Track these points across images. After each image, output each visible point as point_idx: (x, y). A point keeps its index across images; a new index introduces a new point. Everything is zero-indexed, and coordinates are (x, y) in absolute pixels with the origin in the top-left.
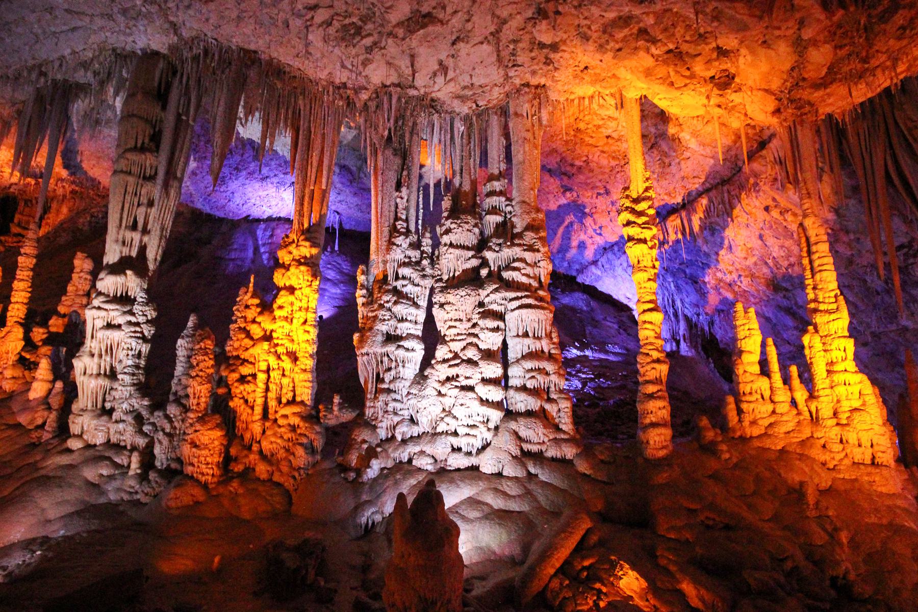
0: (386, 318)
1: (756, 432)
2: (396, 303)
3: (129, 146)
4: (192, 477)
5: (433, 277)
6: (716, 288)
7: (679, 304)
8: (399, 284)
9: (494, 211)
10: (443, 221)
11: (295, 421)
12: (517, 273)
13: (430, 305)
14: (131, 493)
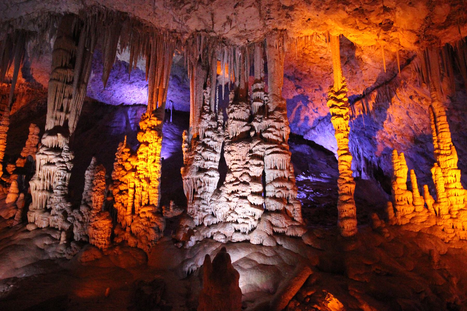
0: (199, 159)
1: (404, 222)
2: (204, 151)
3: (58, 66)
4: (94, 245)
5: (224, 136)
6: (382, 142)
7: (361, 151)
8: (205, 140)
9: (258, 100)
10: (229, 105)
11: (149, 215)
12: (271, 134)
13: (223, 152)
14: (61, 254)
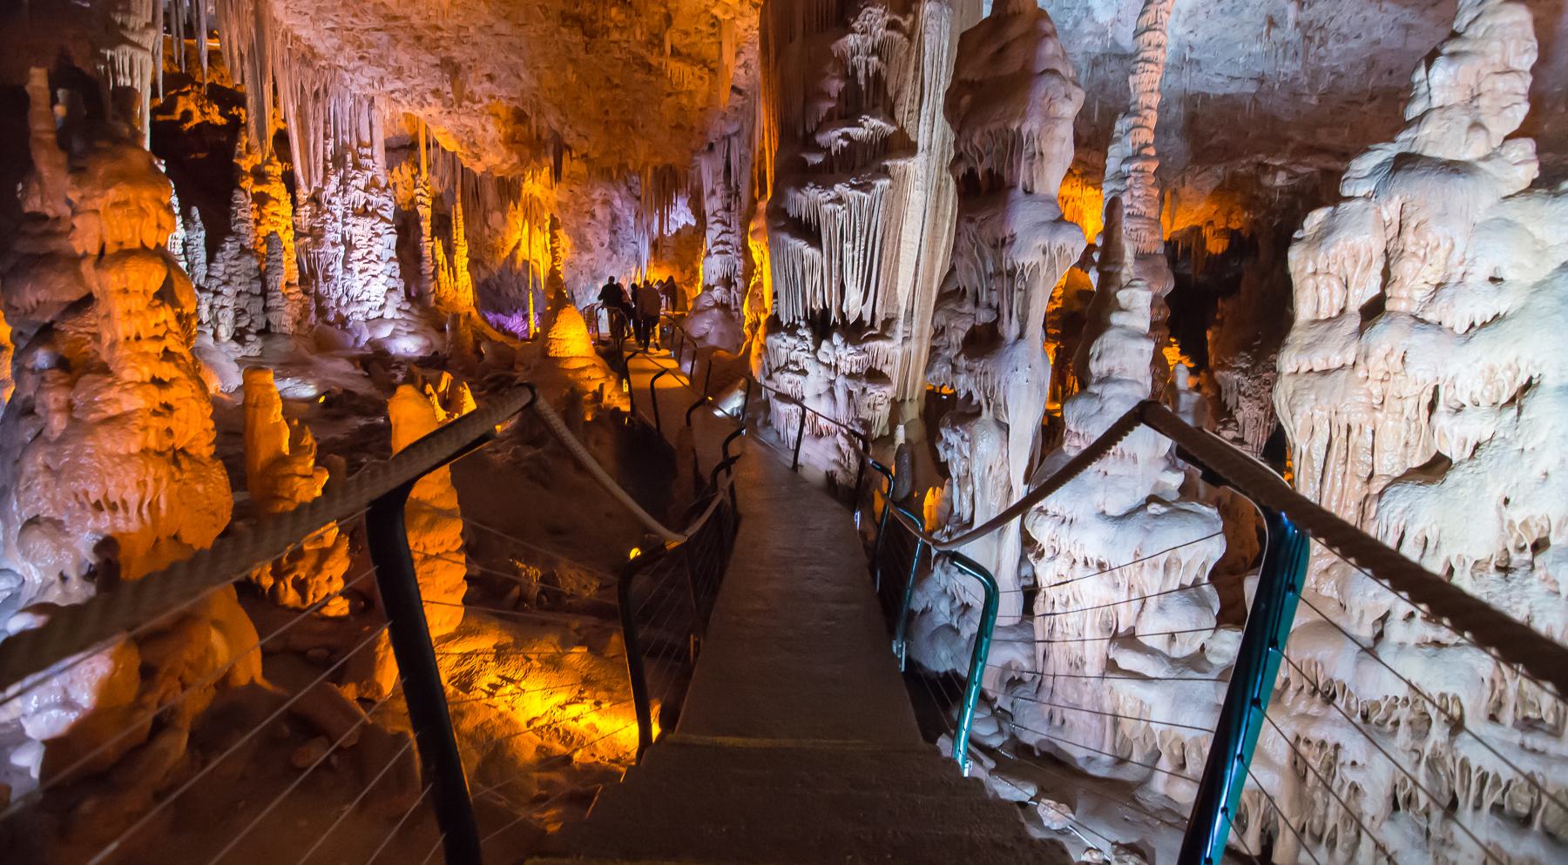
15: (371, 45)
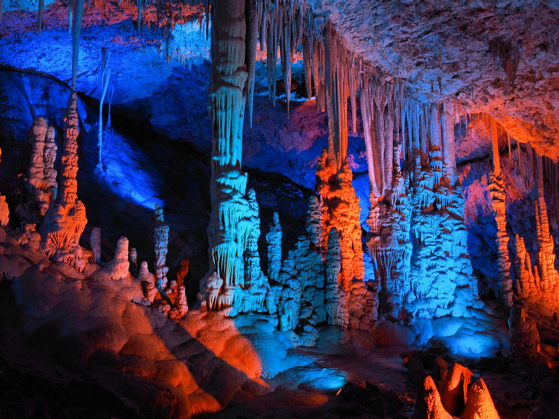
0: (399, 228)
11: (365, 291)
15: (425, 50)
